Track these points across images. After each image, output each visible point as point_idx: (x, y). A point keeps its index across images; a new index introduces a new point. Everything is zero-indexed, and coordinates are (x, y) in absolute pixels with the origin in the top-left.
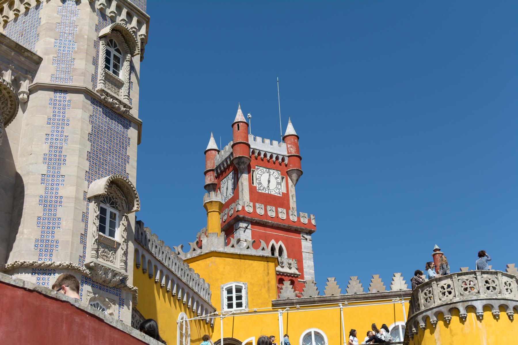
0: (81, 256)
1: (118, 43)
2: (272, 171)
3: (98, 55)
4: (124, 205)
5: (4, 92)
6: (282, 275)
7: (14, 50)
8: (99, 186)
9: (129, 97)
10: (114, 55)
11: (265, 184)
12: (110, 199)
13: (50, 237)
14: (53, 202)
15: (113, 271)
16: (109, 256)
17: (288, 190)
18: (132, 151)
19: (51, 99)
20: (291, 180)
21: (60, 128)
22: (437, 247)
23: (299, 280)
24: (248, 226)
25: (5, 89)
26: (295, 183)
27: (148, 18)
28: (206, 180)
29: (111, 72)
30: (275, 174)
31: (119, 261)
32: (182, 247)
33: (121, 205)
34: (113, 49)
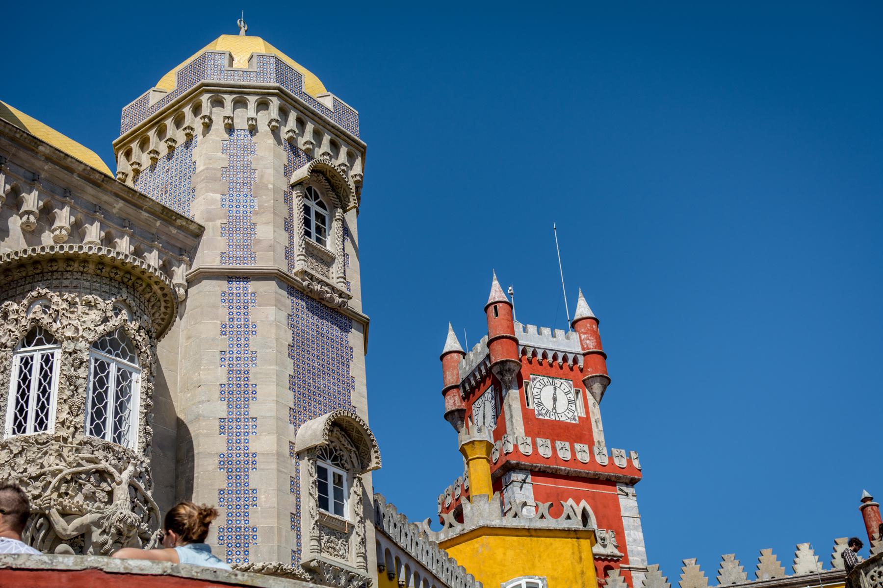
0: (294, 552)
1: (323, 192)
2: (558, 382)
3: (291, 215)
4: (354, 460)
5: (155, 288)
6: (610, 561)
7: (159, 218)
8: (314, 430)
9: (345, 279)
10: (316, 213)
11: (548, 404)
12: (331, 453)
13: (243, 522)
14: (242, 463)
15: (348, 572)
16: (337, 548)
17: (587, 412)
18: (358, 368)
19: (224, 293)
20: (592, 394)
21: (243, 340)
22: (866, 494)
23: (621, 565)
24: (527, 477)
25: (156, 283)
26: (598, 400)
27: (364, 147)
28: (447, 405)
29: (313, 241)
30: (565, 386)
31: (354, 555)
32: (430, 522)
33: (349, 461)
34: (314, 203)
